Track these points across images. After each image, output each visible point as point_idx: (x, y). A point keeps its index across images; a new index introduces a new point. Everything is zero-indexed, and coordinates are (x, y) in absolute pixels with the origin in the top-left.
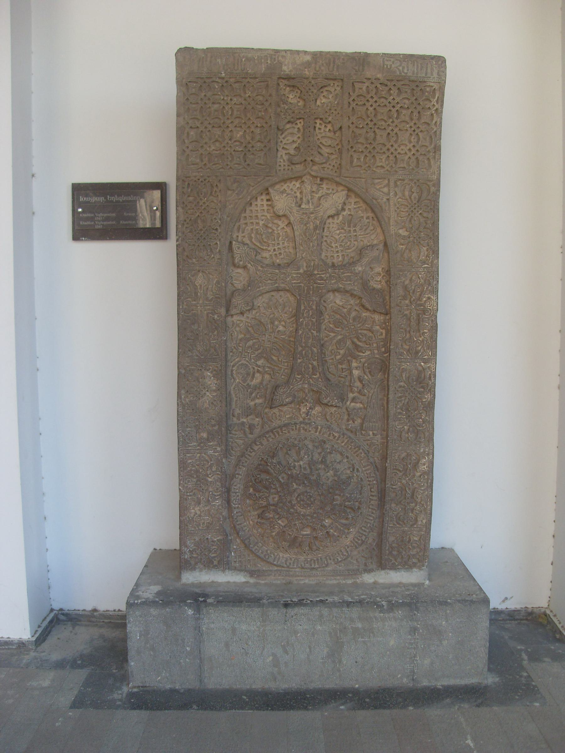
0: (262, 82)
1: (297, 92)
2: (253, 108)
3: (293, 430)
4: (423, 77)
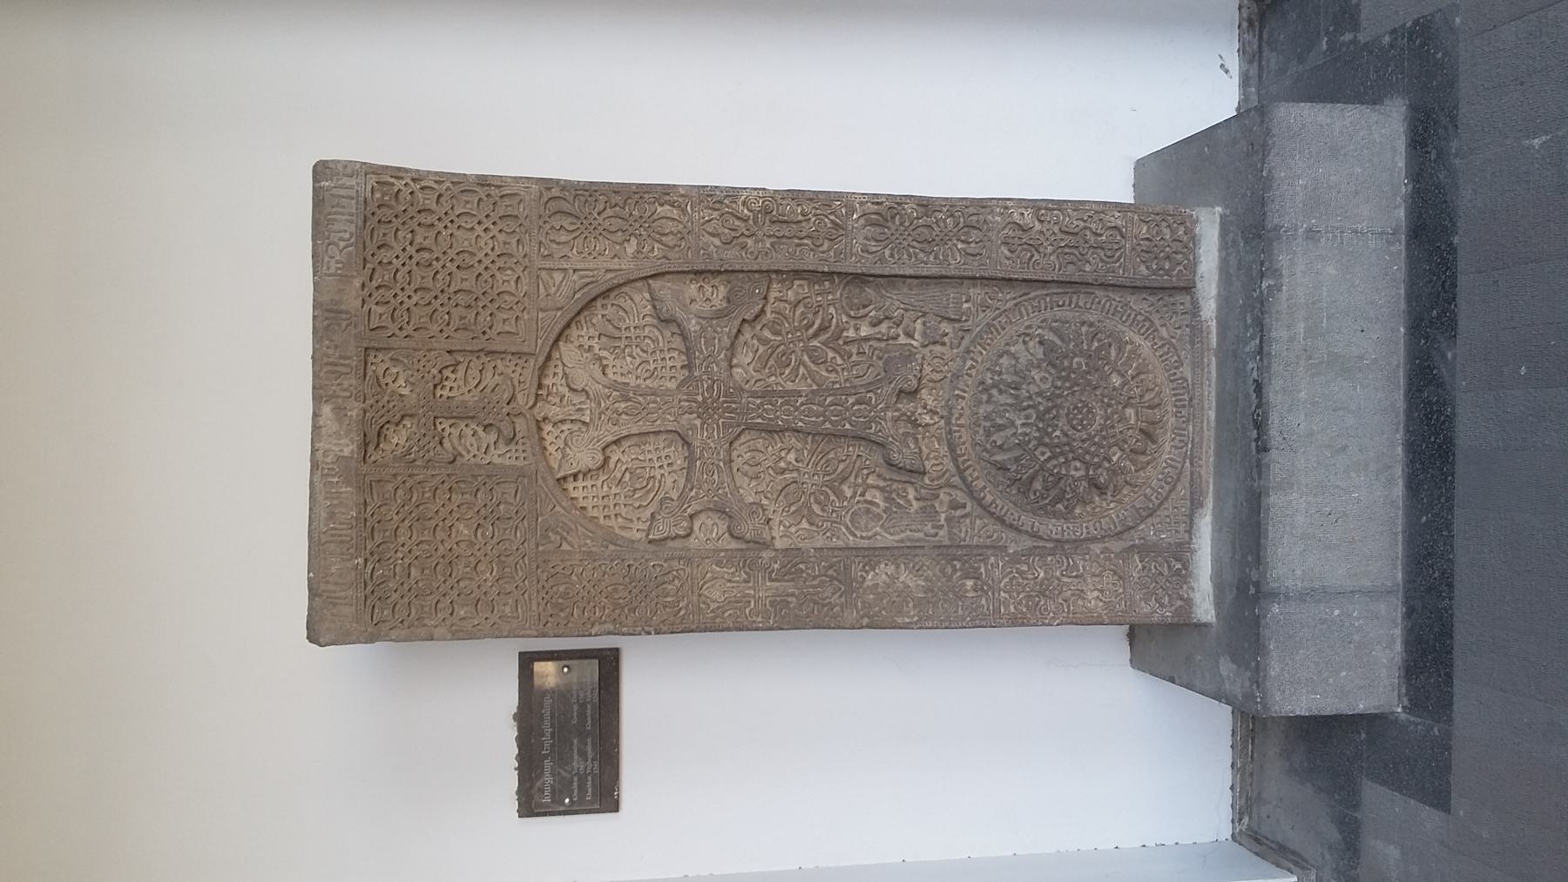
3: (960, 437)
4: (357, 203)
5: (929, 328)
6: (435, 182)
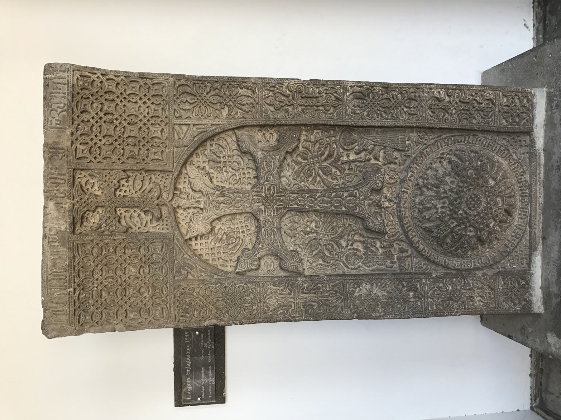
0: (78, 250)
1: (88, 214)
2: (105, 258)
3: (405, 214)
4: (68, 87)
5: (388, 155)
6: (115, 76)
